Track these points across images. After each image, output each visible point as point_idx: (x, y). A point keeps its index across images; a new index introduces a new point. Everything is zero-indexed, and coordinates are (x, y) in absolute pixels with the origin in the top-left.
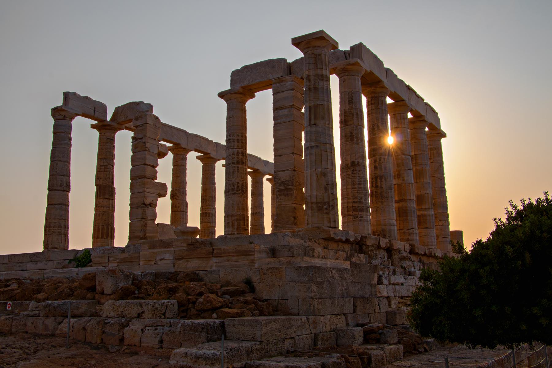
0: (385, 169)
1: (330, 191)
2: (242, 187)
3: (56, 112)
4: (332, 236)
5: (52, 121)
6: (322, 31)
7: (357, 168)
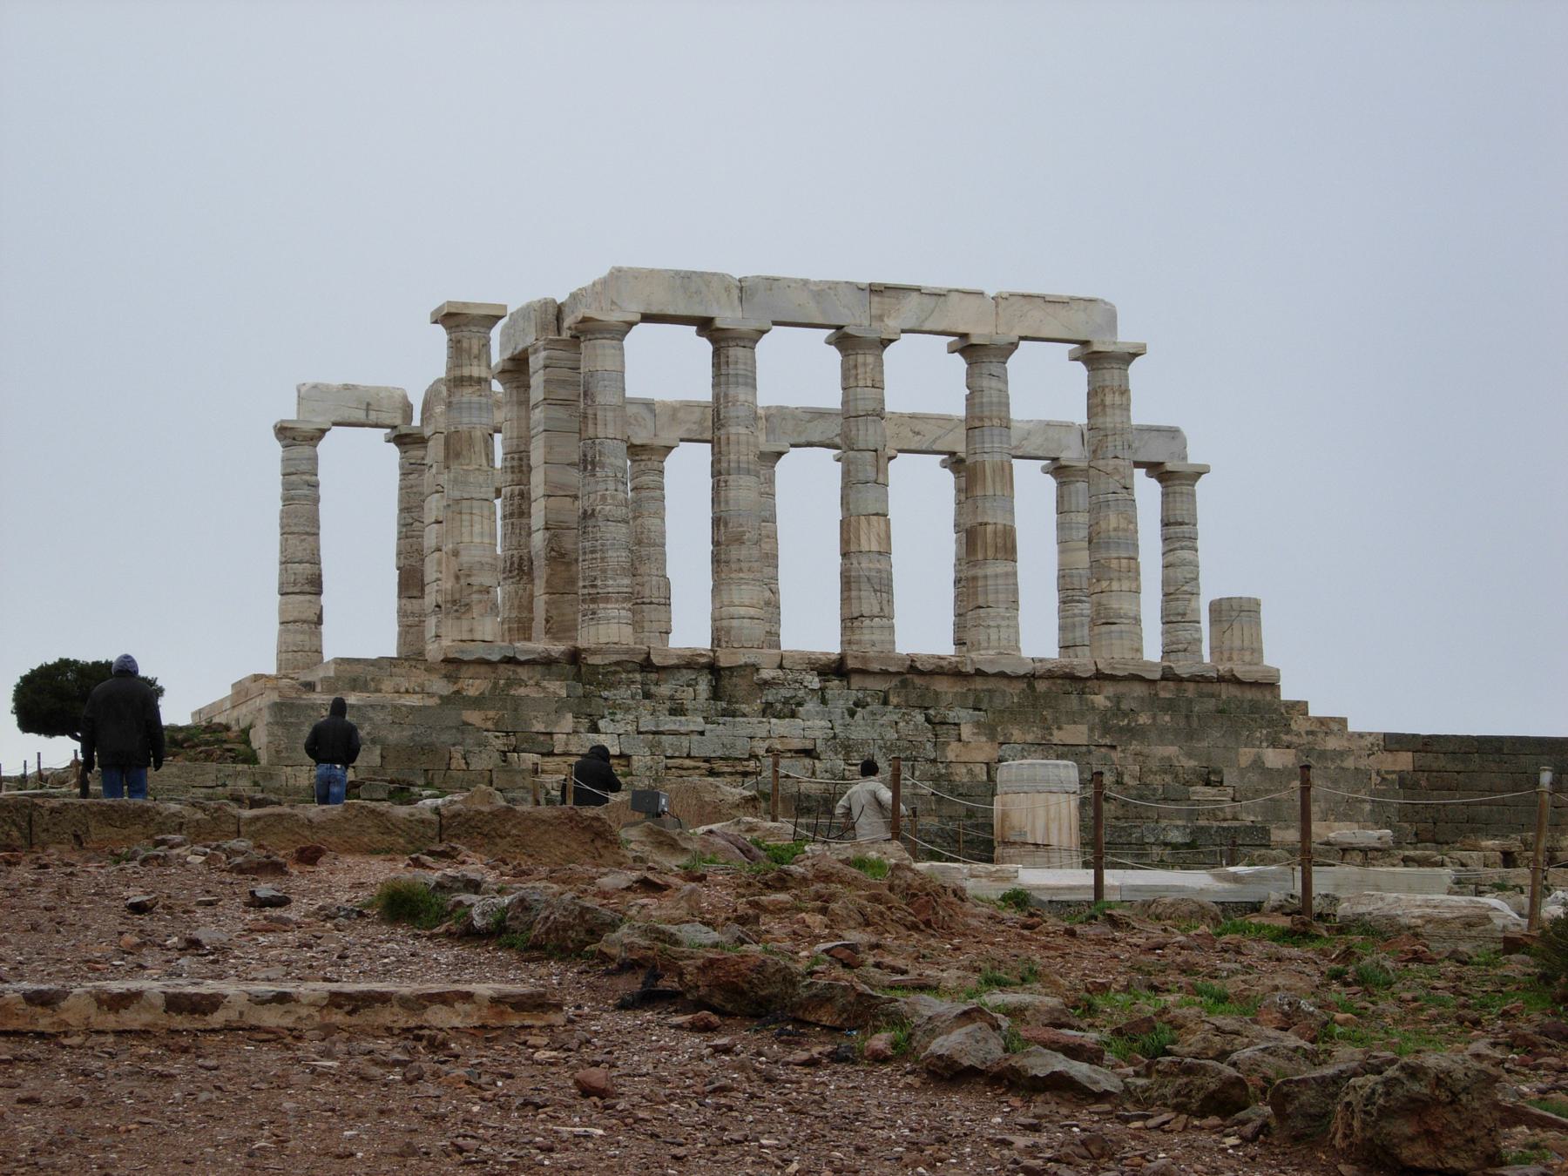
0: (727, 502)
1: (463, 582)
2: (520, 565)
3: (284, 432)
4: (451, 656)
5: (276, 449)
6: (449, 302)
7: (591, 522)
